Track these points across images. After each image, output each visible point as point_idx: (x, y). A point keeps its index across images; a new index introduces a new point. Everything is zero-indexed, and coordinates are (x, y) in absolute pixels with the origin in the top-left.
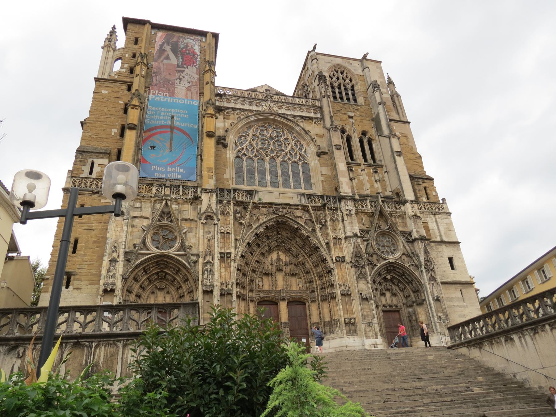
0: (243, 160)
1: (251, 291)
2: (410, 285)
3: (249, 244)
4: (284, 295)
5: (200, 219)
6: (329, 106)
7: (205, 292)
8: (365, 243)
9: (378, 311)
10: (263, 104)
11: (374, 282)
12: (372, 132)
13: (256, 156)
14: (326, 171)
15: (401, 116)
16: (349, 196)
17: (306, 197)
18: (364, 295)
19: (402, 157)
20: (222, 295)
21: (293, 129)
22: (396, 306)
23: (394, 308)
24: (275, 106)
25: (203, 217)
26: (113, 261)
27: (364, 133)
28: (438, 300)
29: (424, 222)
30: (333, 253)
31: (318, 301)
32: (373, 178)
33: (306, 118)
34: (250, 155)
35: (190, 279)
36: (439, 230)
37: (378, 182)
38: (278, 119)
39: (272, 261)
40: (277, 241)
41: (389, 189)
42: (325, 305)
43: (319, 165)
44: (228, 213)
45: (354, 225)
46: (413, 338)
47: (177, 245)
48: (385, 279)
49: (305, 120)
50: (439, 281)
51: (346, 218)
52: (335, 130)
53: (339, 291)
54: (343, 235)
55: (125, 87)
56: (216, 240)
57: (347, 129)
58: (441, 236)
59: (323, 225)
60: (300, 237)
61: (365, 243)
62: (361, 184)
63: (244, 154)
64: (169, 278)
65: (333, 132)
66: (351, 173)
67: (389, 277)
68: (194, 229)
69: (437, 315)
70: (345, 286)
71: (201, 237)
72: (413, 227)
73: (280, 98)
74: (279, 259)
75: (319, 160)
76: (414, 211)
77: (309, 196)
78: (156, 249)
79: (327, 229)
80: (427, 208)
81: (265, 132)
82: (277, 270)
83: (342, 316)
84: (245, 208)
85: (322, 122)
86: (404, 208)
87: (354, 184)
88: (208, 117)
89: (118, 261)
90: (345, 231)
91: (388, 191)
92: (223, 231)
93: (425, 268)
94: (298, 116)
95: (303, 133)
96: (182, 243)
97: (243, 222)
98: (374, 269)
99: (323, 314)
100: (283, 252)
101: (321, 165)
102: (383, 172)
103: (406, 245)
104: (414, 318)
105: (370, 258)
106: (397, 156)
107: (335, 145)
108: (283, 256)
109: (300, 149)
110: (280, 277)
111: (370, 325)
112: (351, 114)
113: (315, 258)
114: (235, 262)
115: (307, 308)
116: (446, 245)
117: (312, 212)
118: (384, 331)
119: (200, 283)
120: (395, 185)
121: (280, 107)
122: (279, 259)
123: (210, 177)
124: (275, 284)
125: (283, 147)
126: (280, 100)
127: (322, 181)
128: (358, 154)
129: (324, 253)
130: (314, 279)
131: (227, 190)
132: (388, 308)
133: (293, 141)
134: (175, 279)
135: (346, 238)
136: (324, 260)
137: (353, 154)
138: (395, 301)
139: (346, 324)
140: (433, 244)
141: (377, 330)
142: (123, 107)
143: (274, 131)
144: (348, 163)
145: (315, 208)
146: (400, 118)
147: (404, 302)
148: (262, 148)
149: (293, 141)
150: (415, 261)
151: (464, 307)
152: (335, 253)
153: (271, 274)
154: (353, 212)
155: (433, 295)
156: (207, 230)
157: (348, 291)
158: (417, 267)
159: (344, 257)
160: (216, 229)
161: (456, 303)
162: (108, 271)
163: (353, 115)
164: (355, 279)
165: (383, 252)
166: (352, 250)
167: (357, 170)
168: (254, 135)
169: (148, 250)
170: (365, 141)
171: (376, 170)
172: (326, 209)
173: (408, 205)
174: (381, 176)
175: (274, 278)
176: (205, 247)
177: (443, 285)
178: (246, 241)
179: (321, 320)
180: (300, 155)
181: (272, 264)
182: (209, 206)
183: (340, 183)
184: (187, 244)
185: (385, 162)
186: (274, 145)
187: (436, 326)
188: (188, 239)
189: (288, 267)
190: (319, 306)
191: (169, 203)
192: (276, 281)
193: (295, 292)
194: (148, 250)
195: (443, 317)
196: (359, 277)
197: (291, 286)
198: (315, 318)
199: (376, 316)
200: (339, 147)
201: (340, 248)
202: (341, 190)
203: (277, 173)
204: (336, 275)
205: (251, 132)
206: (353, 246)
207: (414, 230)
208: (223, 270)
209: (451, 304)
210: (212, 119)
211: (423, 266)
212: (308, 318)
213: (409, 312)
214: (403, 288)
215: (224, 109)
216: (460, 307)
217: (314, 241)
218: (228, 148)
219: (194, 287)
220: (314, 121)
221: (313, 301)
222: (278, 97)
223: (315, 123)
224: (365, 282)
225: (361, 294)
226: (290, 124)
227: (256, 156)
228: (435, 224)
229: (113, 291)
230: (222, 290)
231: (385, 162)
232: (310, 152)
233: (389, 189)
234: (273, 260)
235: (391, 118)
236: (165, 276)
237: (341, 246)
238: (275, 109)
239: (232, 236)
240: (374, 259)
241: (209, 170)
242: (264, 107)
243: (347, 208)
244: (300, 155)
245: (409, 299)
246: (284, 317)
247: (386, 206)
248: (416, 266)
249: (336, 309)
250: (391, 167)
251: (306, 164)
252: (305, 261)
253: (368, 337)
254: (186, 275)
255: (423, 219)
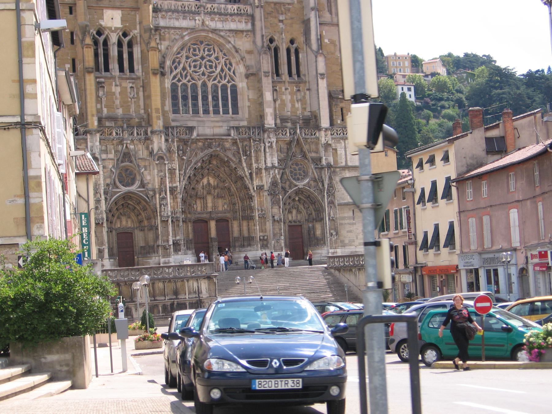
0: (178, 86)
1: (190, 213)
2: (313, 205)
3: (189, 177)
4: (213, 216)
5: (154, 160)
6: (261, 20)
7: (162, 221)
8: (281, 171)
9: (285, 226)
10: (197, 18)
11: (285, 204)
12: (301, 39)
13: (189, 81)
14: (252, 95)
15: (334, 16)
16: (272, 129)
17: (235, 130)
18: (276, 218)
19: (325, 80)
20: (172, 221)
21: (225, 45)
22: (299, 222)
23: (298, 223)
24: (207, 18)
25: (157, 157)
26: (98, 201)
27: (292, 42)
28: (332, 220)
29: (334, 148)
30: (255, 182)
31: (240, 220)
32: (295, 96)
33: (236, 32)
34: (185, 81)
35: (149, 209)
36: (346, 155)
37: (299, 102)
38: (210, 35)
39: (203, 186)
40: (208, 169)
41: (308, 109)
42: (245, 223)
43: (246, 89)
44: (173, 150)
45: (274, 156)
46: (309, 247)
47: (137, 183)
48: (294, 200)
49: (236, 33)
50: (336, 202)
51: (267, 150)
52: (265, 53)
53: (257, 215)
54: (264, 165)
55: (68, 10)
56: (167, 178)
57: (276, 38)
58: (346, 161)
59: (248, 156)
60: (229, 167)
61: (281, 171)
62: (283, 103)
63: (179, 78)
64: (131, 207)
65: (263, 55)
66: (275, 93)
67: (297, 199)
68: (148, 167)
69: (329, 232)
70: (262, 210)
71: (156, 176)
72: (324, 155)
73: (212, 6)
74: (209, 184)
75: (247, 83)
76: (327, 139)
77: (237, 128)
78: (122, 186)
79: (251, 159)
80: (339, 133)
81: (197, 52)
82: (208, 193)
83: (258, 234)
84: (185, 144)
85: (252, 35)
86: (319, 134)
87: (277, 106)
88: (152, 50)
89: (100, 200)
90: (265, 161)
91: (307, 111)
92: (170, 168)
93: (327, 193)
94: (230, 31)
95: (233, 51)
96: (142, 181)
97: (184, 158)
98: (286, 195)
99: (243, 231)
100: (213, 178)
101: (248, 88)
102: (306, 89)
103: (314, 171)
104: (312, 232)
105: (284, 185)
106: (321, 78)
107: (264, 72)
108: (212, 181)
109: (229, 70)
110: (209, 199)
111: (278, 241)
112: (281, 18)
113: (239, 184)
114: (180, 195)
115: (230, 225)
116: (349, 170)
117: (240, 145)
118: (288, 243)
119: (158, 214)
120: (315, 108)
121: (212, 20)
122: (209, 184)
123: (158, 118)
124: (205, 206)
125: (214, 67)
126: (212, 9)
127: (249, 107)
128: (284, 69)
129: (247, 182)
130: (237, 201)
131: (171, 127)
132: (293, 224)
133: (223, 58)
134: (135, 208)
135: (266, 169)
136: (247, 188)
137: (279, 67)
138: (299, 218)
139: (260, 239)
140: (338, 169)
141: (283, 245)
142: (70, 37)
143: (205, 48)
144: (273, 82)
145: (242, 140)
146: (332, 18)
147: (306, 218)
148: (196, 72)
149: (223, 58)
150: (320, 186)
151: (353, 224)
152: (256, 182)
153: (203, 198)
154: (274, 144)
155: (329, 215)
156: (159, 169)
157: (264, 214)
158: (321, 191)
159: (263, 186)
160: (167, 168)
161: (346, 221)
162: (97, 208)
163: (284, 18)
164: (270, 205)
165: (294, 179)
166: (270, 180)
167: (280, 88)
168: (187, 57)
169: (117, 187)
170: (293, 51)
171: (299, 89)
172: (252, 141)
173: (323, 133)
174: (303, 94)
175: (205, 201)
176: (159, 184)
177: (339, 207)
178: (188, 176)
179: (241, 235)
180: (230, 76)
181: (203, 189)
182: (160, 149)
183: (265, 114)
184: (145, 182)
185: (308, 77)
186: (206, 67)
187: (327, 241)
188: (145, 176)
189: (216, 190)
190: (240, 225)
191: (128, 145)
192: (206, 203)
193: (221, 212)
194: (117, 187)
195: (334, 233)
196: (273, 203)
197: (218, 207)
198: (236, 234)
199: (283, 234)
200: (267, 74)
201: (260, 176)
202: (266, 122)
203: (207, 98)
204: (256, 201)
205: (184, 53)
206: (271, 177)
207: (324, 158)
208: (172, 201)
209: (343, 222)
210: (154, 52)
211: (326, 192)
212: (231, 233)
213: (309, 227)
214: (307, 207)
215: (160, 28)
216: (349, 224)
217: (240, 172)
218: (166, 77)
219: (152, 216)
220: (245, 34)
221: (235, 219)
222: (211, 5)
223: (245, 36)
224: (277, 207)
225: (274, 217)
226: (221, 40)
227: (189, 81)
228: (343, 149)
229: (102, 223)
230: (172, 217)
231: (308, 77)
232: (239, 72)
233: (308, 109)
234: (204, 185)
235: (323, 19)
236: (127, 206)
237: (261, 175)
238: (207, 23)
239: (177, 171)
240: (287, 186)
241: (157, 110)
242: (197, 22)
243: (269, 140)
244: (230, 76)
245: (311, 216)
246: (213, 233)
247: (303, 133)
248: (321, 190)
249: (253, 228)
250: (313, 87)
251: (234, 89)
252: (230, 186)
253: (276, 251)
254: (145, 206)
255: (333, 145)
